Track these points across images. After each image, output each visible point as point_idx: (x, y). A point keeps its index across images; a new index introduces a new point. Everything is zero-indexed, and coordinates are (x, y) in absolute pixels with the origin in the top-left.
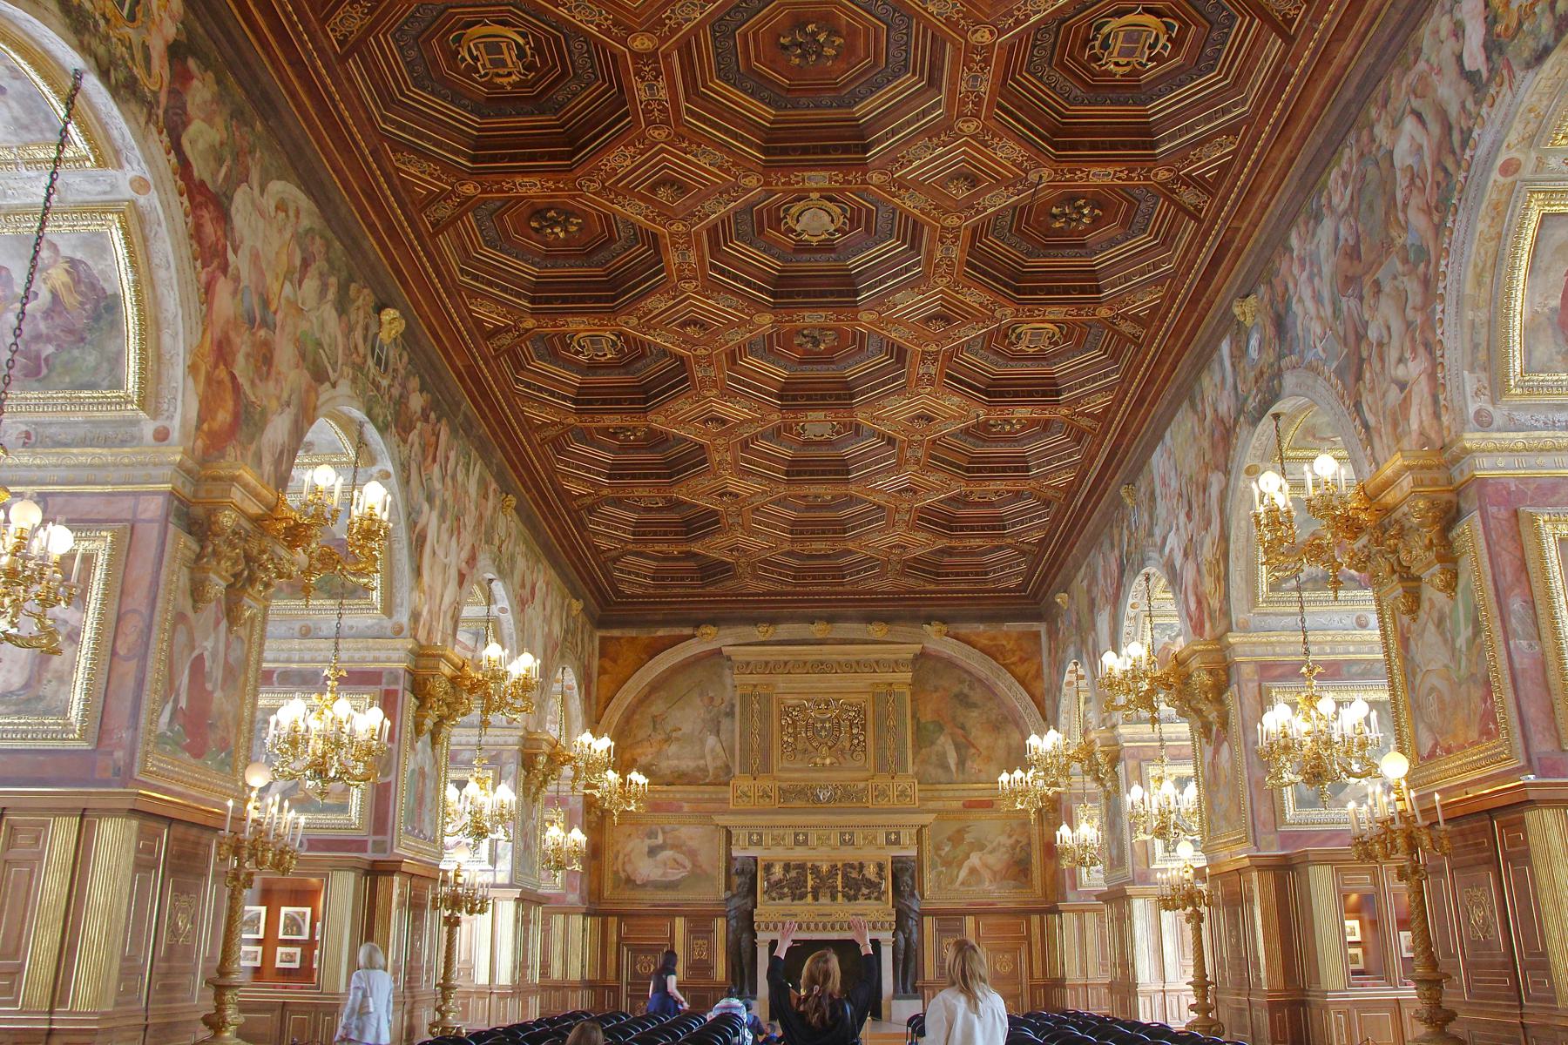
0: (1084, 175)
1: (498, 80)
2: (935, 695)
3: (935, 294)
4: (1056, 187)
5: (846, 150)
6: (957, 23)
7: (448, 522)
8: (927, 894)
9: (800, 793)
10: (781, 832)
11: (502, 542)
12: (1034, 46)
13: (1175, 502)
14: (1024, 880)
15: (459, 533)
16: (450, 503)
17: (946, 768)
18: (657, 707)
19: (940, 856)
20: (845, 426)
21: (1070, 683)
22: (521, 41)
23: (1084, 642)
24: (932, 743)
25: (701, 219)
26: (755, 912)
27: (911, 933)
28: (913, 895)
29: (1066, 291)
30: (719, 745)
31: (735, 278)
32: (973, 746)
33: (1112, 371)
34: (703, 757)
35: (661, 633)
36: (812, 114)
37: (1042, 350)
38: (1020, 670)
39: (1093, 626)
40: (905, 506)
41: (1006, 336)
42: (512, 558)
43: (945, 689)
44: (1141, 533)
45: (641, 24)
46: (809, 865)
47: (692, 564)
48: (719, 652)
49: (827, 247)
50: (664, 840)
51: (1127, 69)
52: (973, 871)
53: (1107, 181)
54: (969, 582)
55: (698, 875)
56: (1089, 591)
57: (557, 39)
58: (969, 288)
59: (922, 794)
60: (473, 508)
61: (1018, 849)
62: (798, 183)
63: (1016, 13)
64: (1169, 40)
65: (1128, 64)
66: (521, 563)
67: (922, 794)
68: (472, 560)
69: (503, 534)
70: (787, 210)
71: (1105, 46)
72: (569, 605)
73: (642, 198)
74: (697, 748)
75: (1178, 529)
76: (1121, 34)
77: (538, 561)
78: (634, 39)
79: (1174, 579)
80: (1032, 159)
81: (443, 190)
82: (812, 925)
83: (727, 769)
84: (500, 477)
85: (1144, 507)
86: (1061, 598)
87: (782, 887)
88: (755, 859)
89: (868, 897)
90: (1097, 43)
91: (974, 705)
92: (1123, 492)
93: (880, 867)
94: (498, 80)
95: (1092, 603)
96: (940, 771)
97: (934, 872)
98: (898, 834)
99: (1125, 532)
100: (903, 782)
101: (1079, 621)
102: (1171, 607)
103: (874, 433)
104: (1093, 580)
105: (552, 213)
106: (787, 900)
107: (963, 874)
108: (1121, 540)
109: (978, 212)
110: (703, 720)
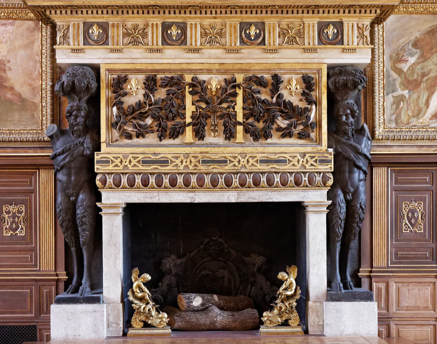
26: (96, 158)
27: (356, 193)
28: (360, 131)
46: (188, 78)
82: (194, 179)
87: (143, 116)
98: (339, 25)
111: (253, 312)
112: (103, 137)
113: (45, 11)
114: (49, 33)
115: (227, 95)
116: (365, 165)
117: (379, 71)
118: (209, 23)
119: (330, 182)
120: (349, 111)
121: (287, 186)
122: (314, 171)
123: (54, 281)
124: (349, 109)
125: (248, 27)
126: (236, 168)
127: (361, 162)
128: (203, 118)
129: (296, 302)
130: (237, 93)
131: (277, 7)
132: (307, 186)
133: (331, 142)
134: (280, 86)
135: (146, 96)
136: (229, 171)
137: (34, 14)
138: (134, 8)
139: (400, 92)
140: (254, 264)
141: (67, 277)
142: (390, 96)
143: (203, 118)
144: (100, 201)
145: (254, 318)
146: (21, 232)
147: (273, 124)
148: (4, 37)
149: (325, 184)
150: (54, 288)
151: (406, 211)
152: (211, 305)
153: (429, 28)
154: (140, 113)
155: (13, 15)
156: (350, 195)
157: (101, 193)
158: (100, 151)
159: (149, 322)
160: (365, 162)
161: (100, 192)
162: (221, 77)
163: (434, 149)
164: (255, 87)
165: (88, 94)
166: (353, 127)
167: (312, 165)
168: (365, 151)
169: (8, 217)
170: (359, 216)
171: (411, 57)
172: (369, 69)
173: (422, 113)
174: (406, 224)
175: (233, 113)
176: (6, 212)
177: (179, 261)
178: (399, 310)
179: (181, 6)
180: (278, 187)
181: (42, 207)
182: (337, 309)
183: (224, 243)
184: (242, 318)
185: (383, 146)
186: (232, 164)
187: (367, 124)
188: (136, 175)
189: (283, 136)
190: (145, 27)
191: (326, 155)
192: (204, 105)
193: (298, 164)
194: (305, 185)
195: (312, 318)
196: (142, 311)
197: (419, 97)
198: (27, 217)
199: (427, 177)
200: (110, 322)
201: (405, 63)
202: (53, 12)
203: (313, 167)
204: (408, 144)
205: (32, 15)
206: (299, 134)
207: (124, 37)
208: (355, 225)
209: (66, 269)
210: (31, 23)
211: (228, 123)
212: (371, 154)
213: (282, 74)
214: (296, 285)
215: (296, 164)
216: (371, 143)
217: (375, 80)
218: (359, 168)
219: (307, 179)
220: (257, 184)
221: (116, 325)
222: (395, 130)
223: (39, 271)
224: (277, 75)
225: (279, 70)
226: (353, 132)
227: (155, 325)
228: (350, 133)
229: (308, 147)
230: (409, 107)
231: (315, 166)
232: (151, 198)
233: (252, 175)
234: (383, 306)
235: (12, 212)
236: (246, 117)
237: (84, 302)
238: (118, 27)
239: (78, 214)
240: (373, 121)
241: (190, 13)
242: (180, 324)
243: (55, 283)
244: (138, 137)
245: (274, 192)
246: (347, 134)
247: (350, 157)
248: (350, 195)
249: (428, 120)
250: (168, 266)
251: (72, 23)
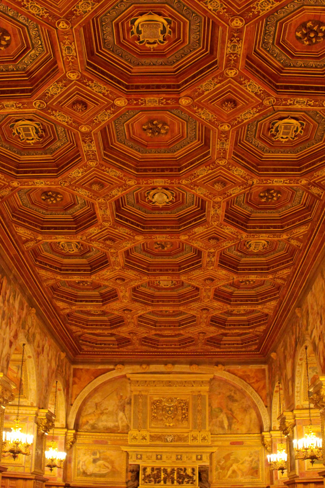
0: (271, 182)
1: (28, 142)
2: (219, 396)
3: (212, 229)
4: (260, 186)
5: (171, 170)
6: (214, 123)
7: (5, 320)
9: (159, 438)
10: (150, 454)
11: (29, 328)
12: (248, 130)
13: (316, 316)
14: (256, 475)
15: (10, 324)
16: (6, 312)
17: (223, 428)
18: (97, 399)
19: (219, 465)
20: (177, 282)
21: (276, 392)
22: (37, 127)
23: (282, 374)
24: (217, 417)
25: (111, 198)
29: (268, 227)
30: (124, 416)
31: (127, 220)
32: (235, 418)
33: (290, 260)
34: (117, 421)
35: (100, 367)
36: (157, 155)
37: (260, 251)
38: (256, 385)
39: (285, 368)
40: (205, 316)
41: (245, 245)
42: (34, 335)
43: (223, 394)
44: (304, 328)
45: (84, 122)
46: (162, 468)
47: (113, 338)
48: (125, 376)
49: (165, 208)
50: (100, 457)
51: (287, 140)
52: (234, 472)
53: (281, 184)
54: (234, 348)
55: (114, 472)
56: (284, 352)
57: (51, 126)
58: (226, 226)
59: (212, 439)
60: (17, 314)
61: (254, 462)
62: (151, 183)
63: (238, 119)
64: (302, 129)
65: (287, 138)
66: (38, 337)
67: (212, 439)
68: (16, 336)
69: (30, 324)
70: (148, 193)
71: (277, 131)
72: (60, 355)
73: (87, 189)
74: (115, 417)
75: (317, 328)
76: (283, 127)
77: (45, 336)
78: (82, 128)
79: (315, 348)
80: (249, 175)
81: (5, 184)
83: (128, 427)
84: (30, 300)
85: (305, 317)
86: (273, 355)
88: (139, 466)
89: (188, 482)
90: (273, 130)
91: (236, 401)
92: (297, 311)
93: (193, 470)
94: (28, 142)
95: (285, 357)
96: (220, 429)
98: (201, 456)
99: (298, 328)
100: (204, 434)
101: (280, 365)
102: (315, 361)
103: (190, 285)
104: (285, 349)
105: (50, 193)
106: (153, 483)
107: (230, 472)
108: (296, 331)
109: (228, 196)
110: (118, 406)
112: (140, 483)
135: (151, 473)
162: (171, 468)
164: (180, 471)
192: (166, 475)
236: (177, 478)
244: (149, 482)
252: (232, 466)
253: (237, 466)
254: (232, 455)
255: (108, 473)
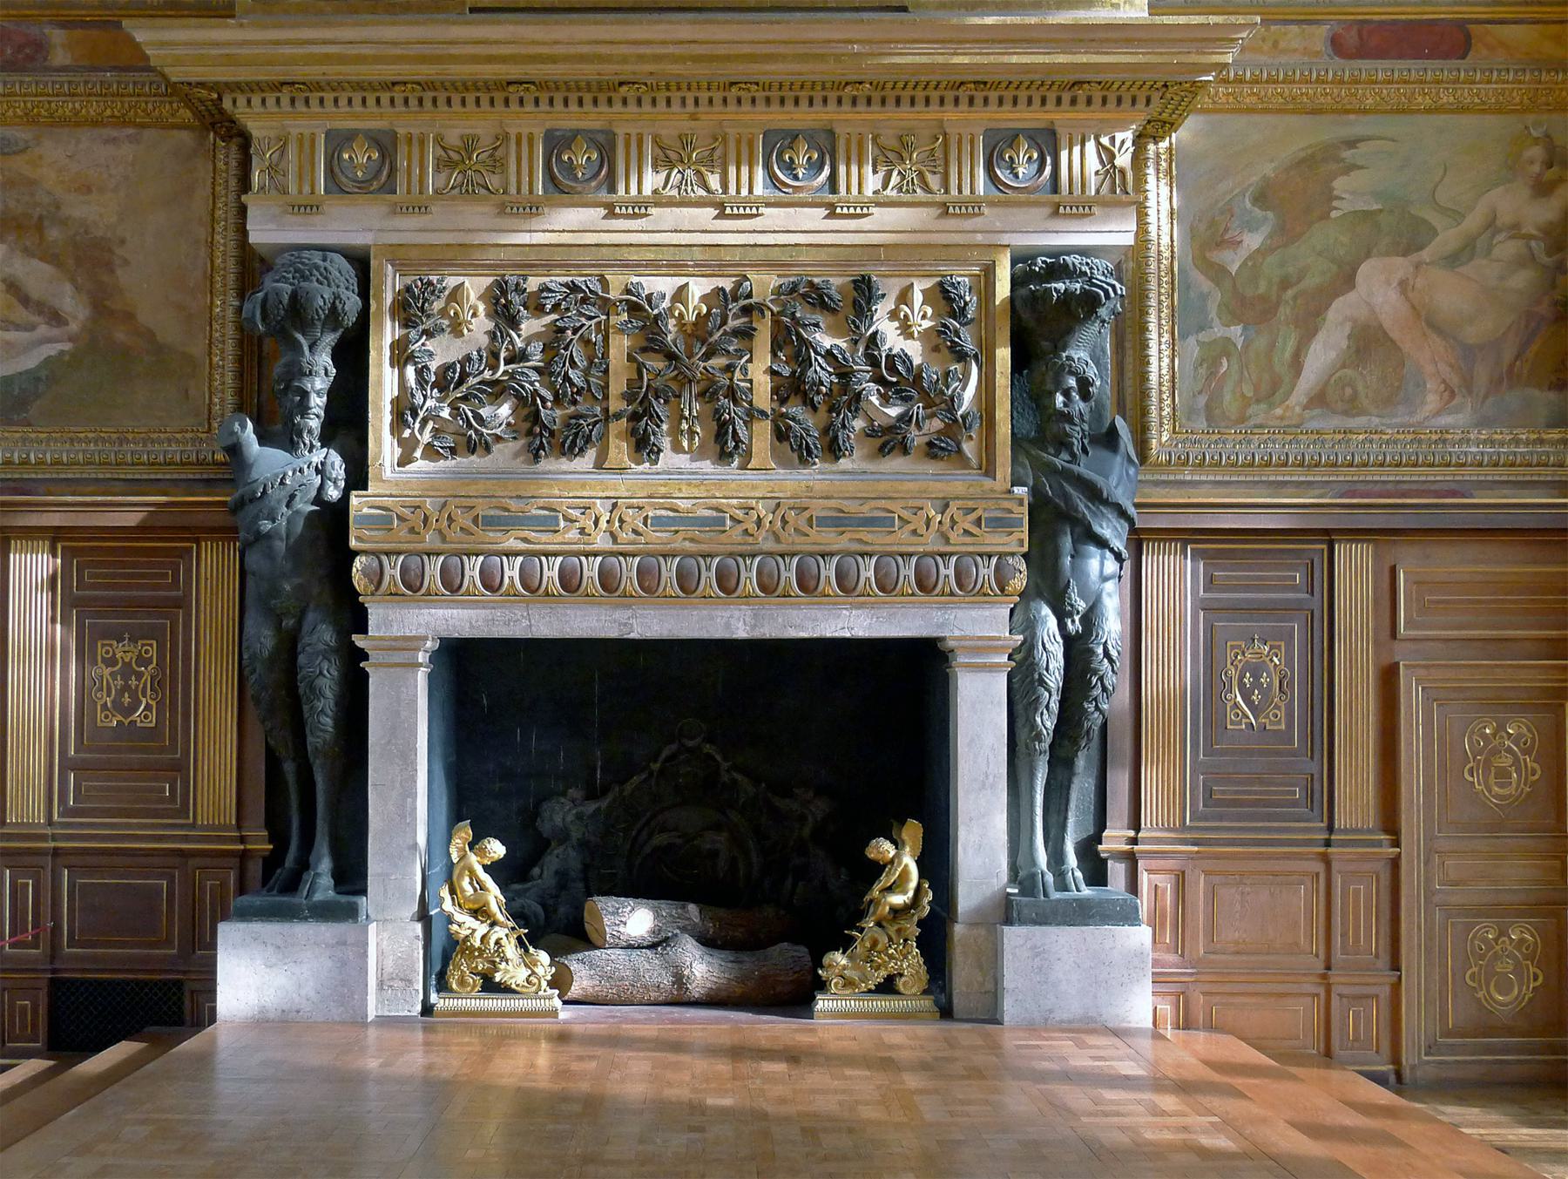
8: (1160, 438)
10: (480, 124)
28: (1109, 439)
97: (1192, 347)
107: (1322, 356)
111: (795, 954)
113: (220, 99)
114: (234, 163)
115: (725, 333)
116: (1119, 536)
117: (1159, 271)
118: (676, 133)
119: (1019, 582)
120: (1072, 382)
121: (894, 593)
122: (971, 549)
123: (235, 857)
124: (1071, 373)
125: (786, 142)
126: (750, 540)
127: (1108, 527)
128: (657, 397)
129: (918, 926)
130: (755, 330)
131: (868, 86)
132: (952, 594)
133: (1021, 471)
134: (876, 310)
136: (730, 548)
137: (192, 111)
138: (467, 90)
139: (1218, 331)
140: (802, 819)
141: (271, 847)
142: (1192, 340)
143: (657, 397)
144: (363, 629)
145: (797, 969)
146: (146, 717)
147: (854, 417)
148: (110, 176)
149: (1002, 590)
150: (232, 877)
151: (1236, 667)
152: (678, 931)
153: (1299, 150)
154: (479, 383)
155: (136, 113)
156: (1077, 618)
157: (366, 608)
158: (366, 489)
159: (498, 977)
160: (1118, 526)
161: (363, 604)
163: (1317, 492)
165: (334, 330)
166: (1086, 427)
167: (966, 532)
168: (1121, 496)
169: (111, 674)
170: (1101, 679)
171: (1249, 231)
172: (1131, 264)
173: (1281, 391)
174: (1236, 705)
175: (742, 384)
176: (104, 660)
177: (591, 807)
178: (1213, 953)
179: (599, 83)
180: (869, 595)
181: (205, 647)
182: (1034, 947)
183: (718, 758)
184: (764, 969)
185: (1171, 482)
186: (740, 528)
187: (1125, 420)
188: (465, 558)
189: (883, 451)
190: (498, 143)
191: (1006, 504)
193: (927, 529)
194: (947, 590)
195: (963, 972)
196: (477, 944)
197: (1272, 346)
198: (164, 674)
199: (1297, 571)
200: (385, 975)
201: (1234, 250)
202: (241, 101)
203: (968, 539)
204: (1242, 478)
205: (188, 114)
206: (930, 444)
207: (437, 169)
208: (1091, 707)
209: (269, 824)
210: (185, 137)
211: (729, 414)
212: (1137, 506)
213: (884, 276)
214: (921, 877)
215: (922, 530)
216: (1137, 473)
217: (1147, 297)
218: (1102, 544)
219: (951, 572)
220: (807, 584)
221: (401, 984)
222: (1206, 437)
223: (193, 826)
224: (869, 278)
225: (875, 265)
226: (1086, 441)
227: (513, 986)
228: (1076, 443)
229: (956, 482)
230: (1246, 373)
231: (972, 534)
232: (507, 623)
233: (795, 560)
234: (1168, 941)
235: (120, 661)
237: (311, 917)
238: (422, 142)
239: (301, 668)
240: (1144, 412)
241: (625, 102)
242: (585, 983)
243: (235, 861)
245: (857, 608)
246: (1068, 446)
247: (1076, 510)
248: (1077, 618)
249: (1298, 410)
250: (558, 820)
251: (294, 132)
252: (1346, 280)
253: (1403, 285)
254: (1351, 168)
255: (52, 371)
